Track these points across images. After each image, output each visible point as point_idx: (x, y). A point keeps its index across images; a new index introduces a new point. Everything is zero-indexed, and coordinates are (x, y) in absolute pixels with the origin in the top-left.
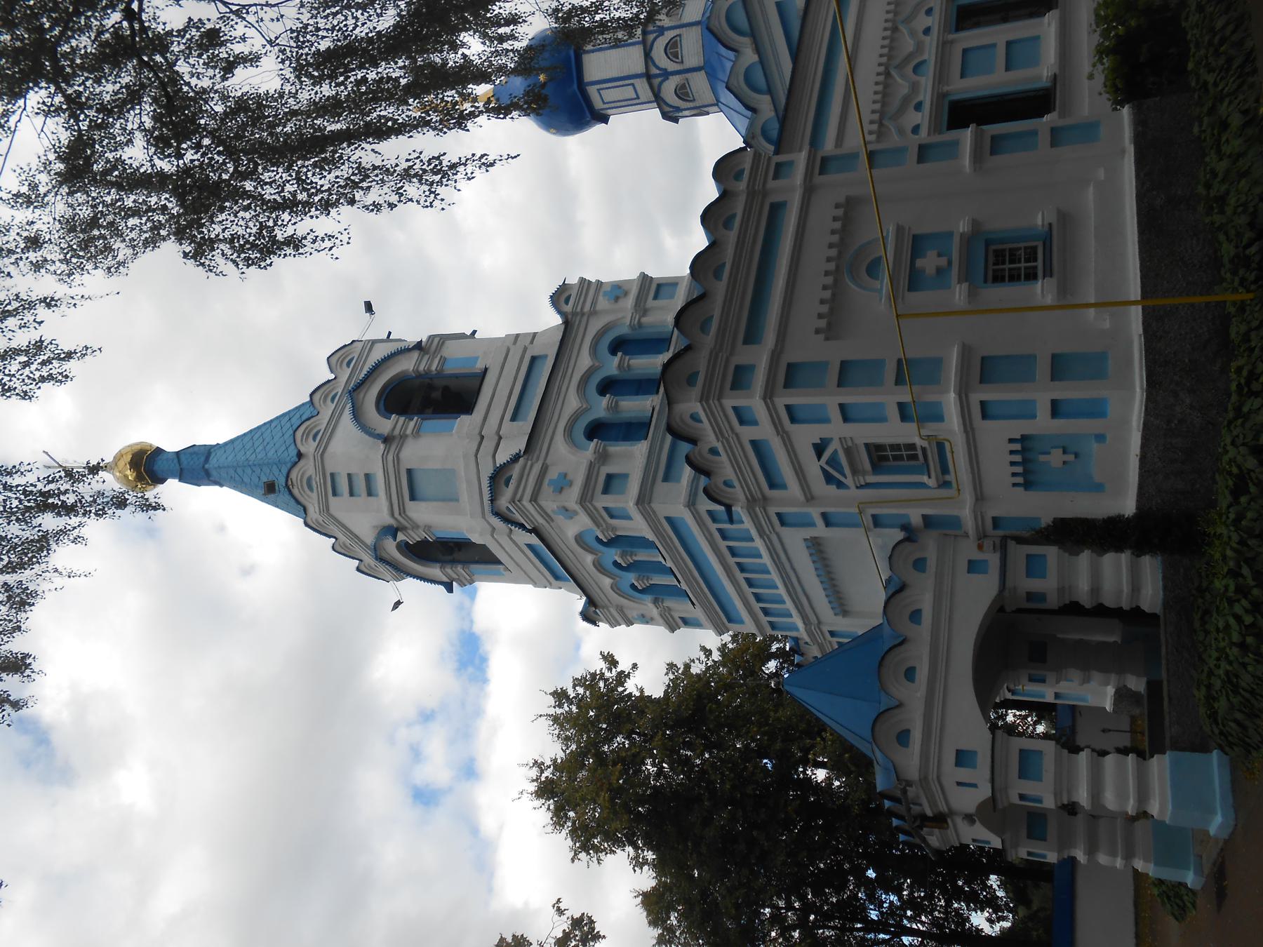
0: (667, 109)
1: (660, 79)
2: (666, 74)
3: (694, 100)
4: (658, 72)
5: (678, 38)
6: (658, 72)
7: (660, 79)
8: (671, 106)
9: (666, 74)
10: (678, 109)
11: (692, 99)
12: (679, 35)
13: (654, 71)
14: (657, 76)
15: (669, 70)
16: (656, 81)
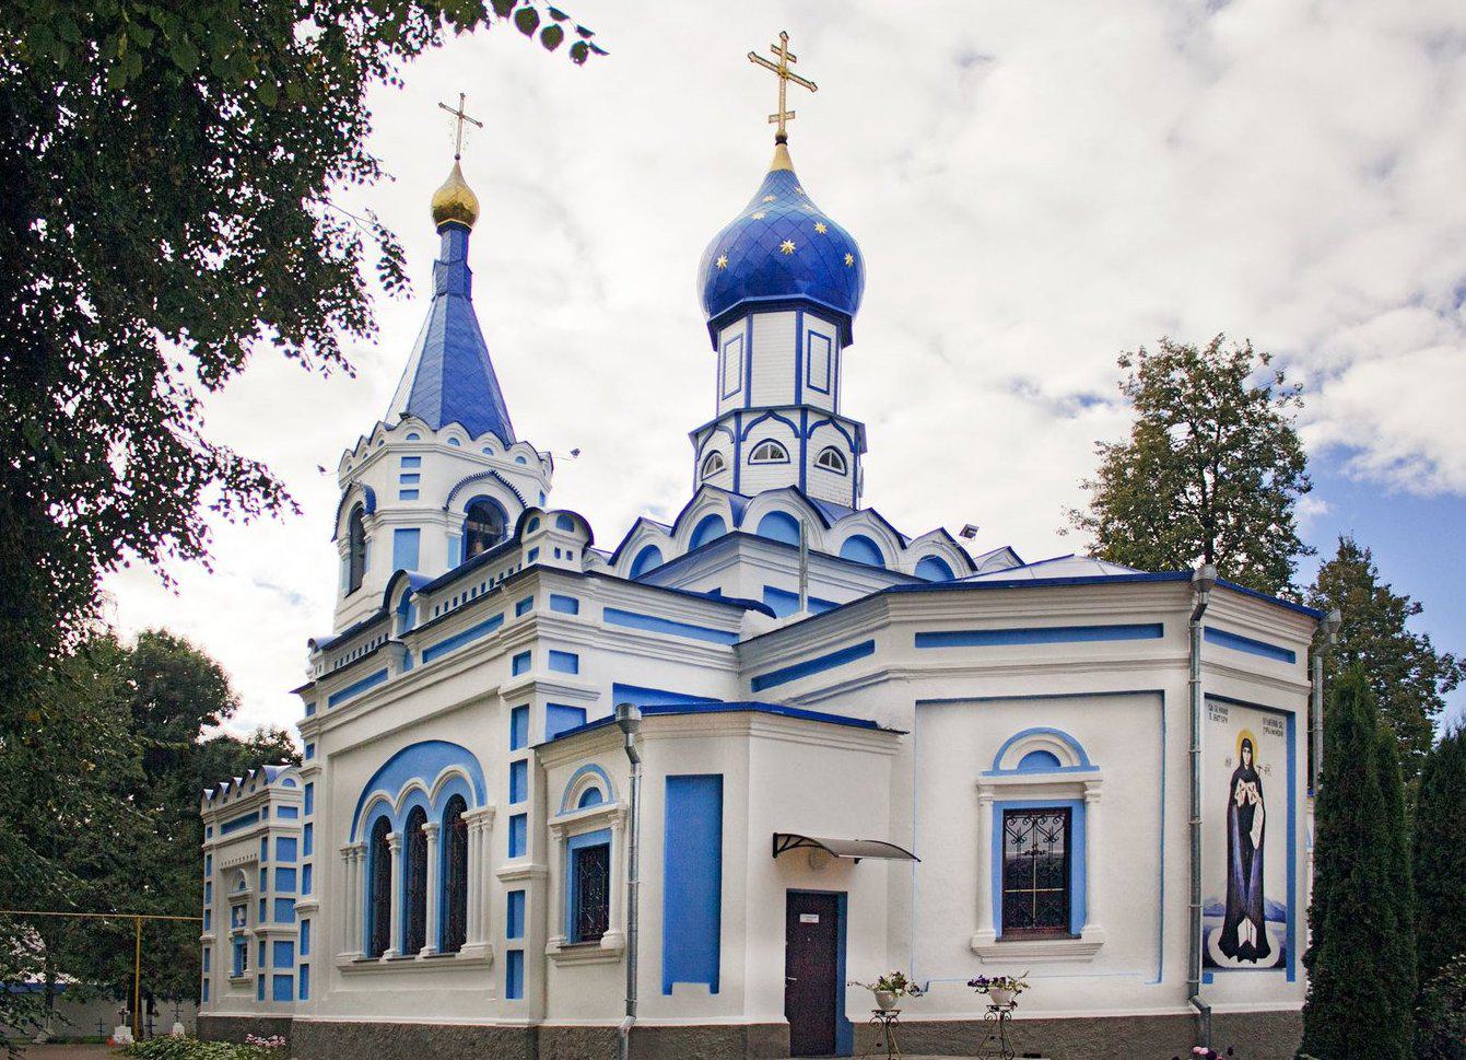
0: (746, 420)
1: (798, 426)
2: (804, 435)
3: (749, 464)
4: (809, 426)
5: (843, 472)
6: (809, 426)
7: (798, 426)
8: (749, 427)
9: (804, 435)
10: (739, 439)
11: (752, 461)
12: (845, 475)
13: (812, 419)
14: (804, 420)
15: (809, 442)
16: (795, 418)
